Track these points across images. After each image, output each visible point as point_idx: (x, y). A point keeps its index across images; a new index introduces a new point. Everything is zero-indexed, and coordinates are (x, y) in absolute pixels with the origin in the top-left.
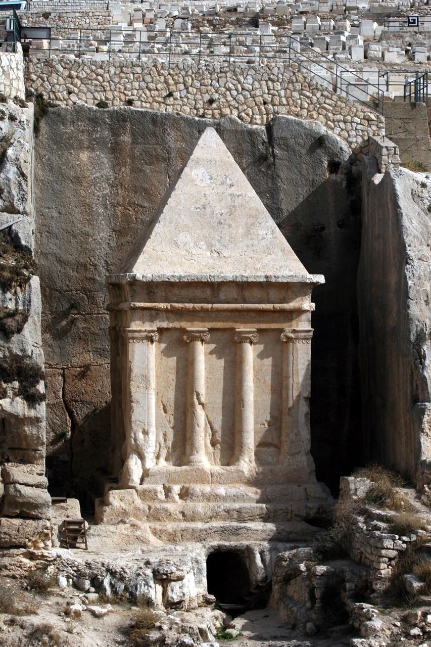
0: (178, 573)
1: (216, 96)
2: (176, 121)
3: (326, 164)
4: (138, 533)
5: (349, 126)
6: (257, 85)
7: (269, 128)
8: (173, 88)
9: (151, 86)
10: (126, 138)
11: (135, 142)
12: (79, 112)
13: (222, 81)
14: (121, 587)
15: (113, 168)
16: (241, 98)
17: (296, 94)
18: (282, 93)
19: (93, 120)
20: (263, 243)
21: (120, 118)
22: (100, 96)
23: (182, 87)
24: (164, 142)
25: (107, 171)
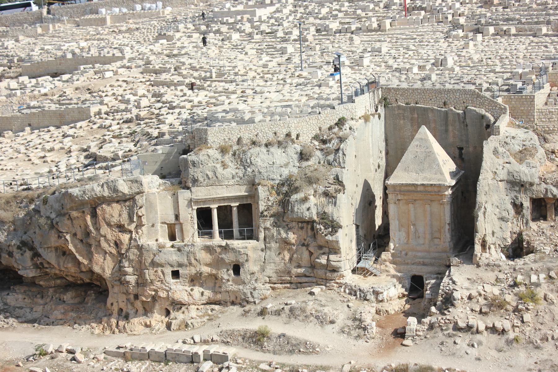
0: (381, 291)
1: (446, 100)
2: (433, 110)
3: (485, 125)
4: (387, 269)
5: (494, 111)
6: (461, 96)
7: (465, 113)
8: (431, 98)
9: (424, 97)
10: (416, 116)
11: (418, 118)
12: (399, 107)
13: (449, 95)
14: (362, 295)
15: (412, 126)
16: (455, 101)
17: (475, 99)
18: (470, 99)
19: (404, 109)
20: (434, 170)
21: (413, 109)
22: (407, 101)
23: (434, 97)
24: (428, 116)
25: (409, 127)
